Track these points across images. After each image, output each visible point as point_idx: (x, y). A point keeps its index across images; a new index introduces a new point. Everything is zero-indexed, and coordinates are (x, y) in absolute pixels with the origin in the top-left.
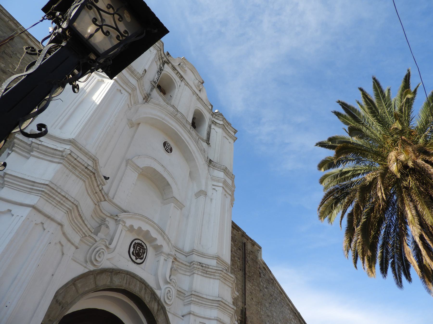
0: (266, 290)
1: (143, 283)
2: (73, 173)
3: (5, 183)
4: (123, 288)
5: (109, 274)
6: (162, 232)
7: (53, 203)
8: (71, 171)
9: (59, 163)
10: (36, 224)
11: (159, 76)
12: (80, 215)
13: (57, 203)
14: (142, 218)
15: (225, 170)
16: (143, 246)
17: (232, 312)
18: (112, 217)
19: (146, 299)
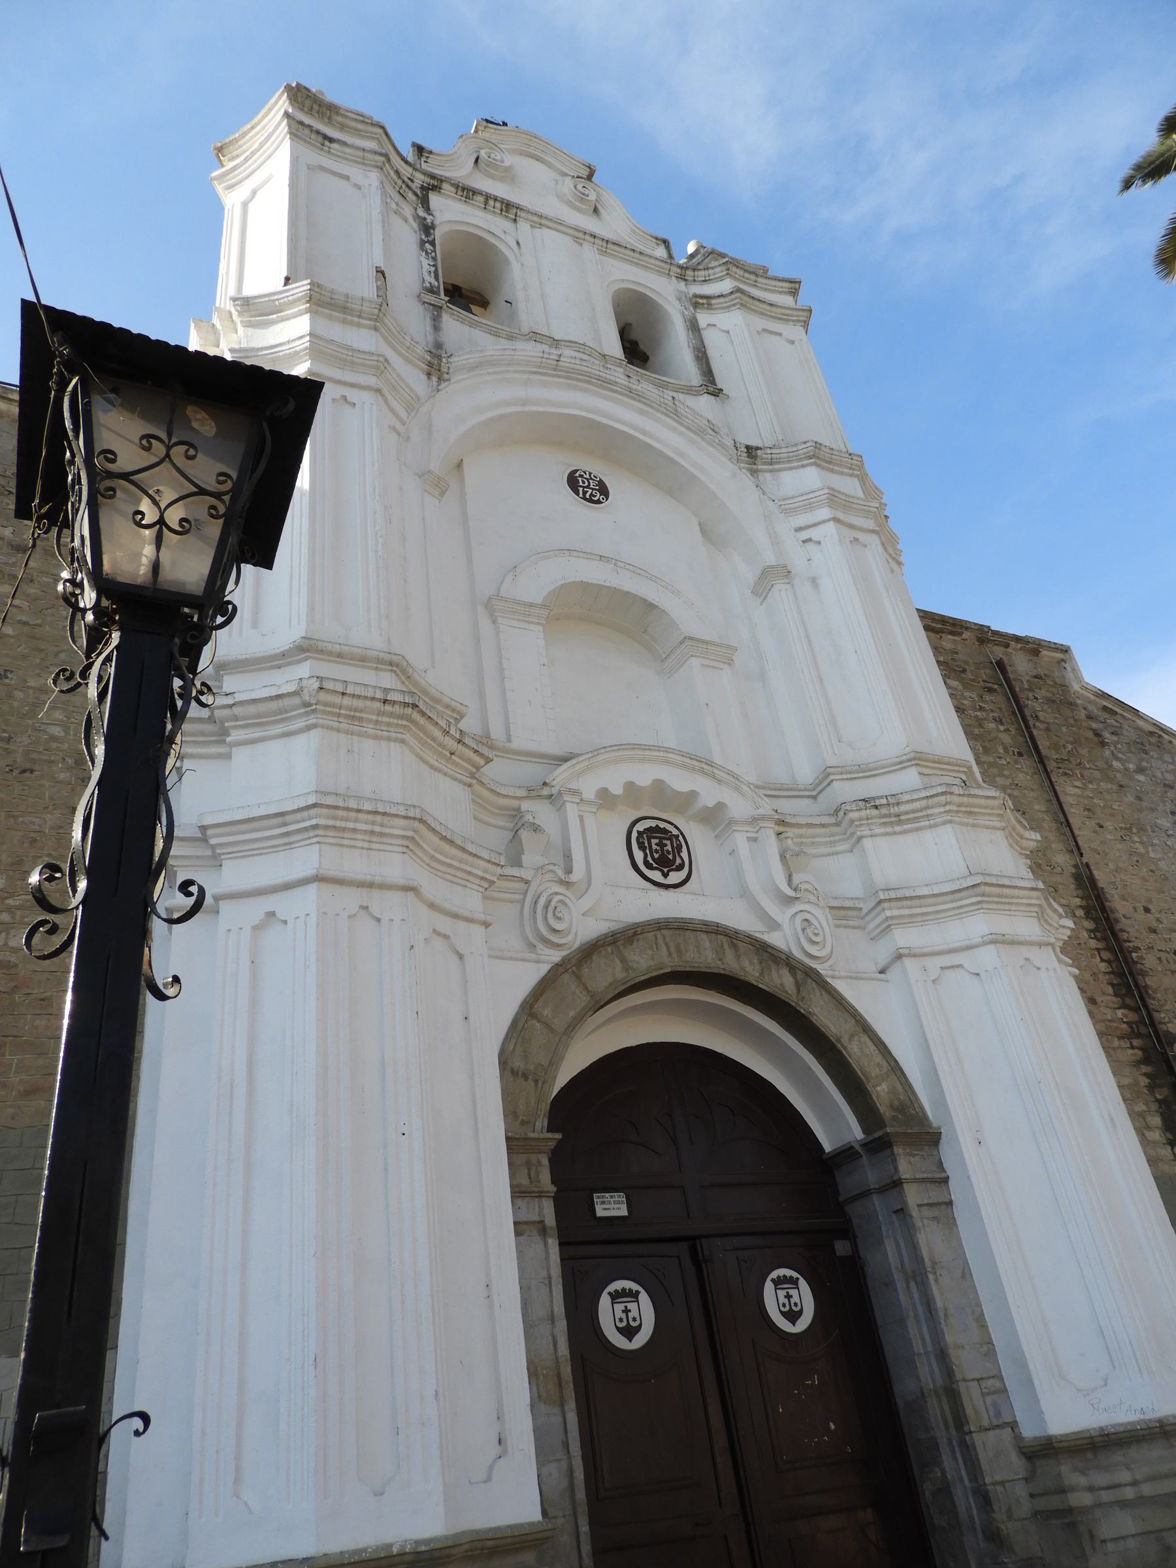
0: (1141, 778)
1: (717, 933)
2: (360, 735)
3: (218, 851)
4: (668, 970)
5: (609, 949)
6: (704, 765)
7: (360, 844)
8: (352, 734)
9: (309, 728)
10: (349, 917)
11: (434, 259)
12: (444, 838)
13: (367, 838)
14: (621, 753)
15: (819, 456)
16: (665, 831)
17: (1036, 899)
18: (535, 793)
19: (749, 970)
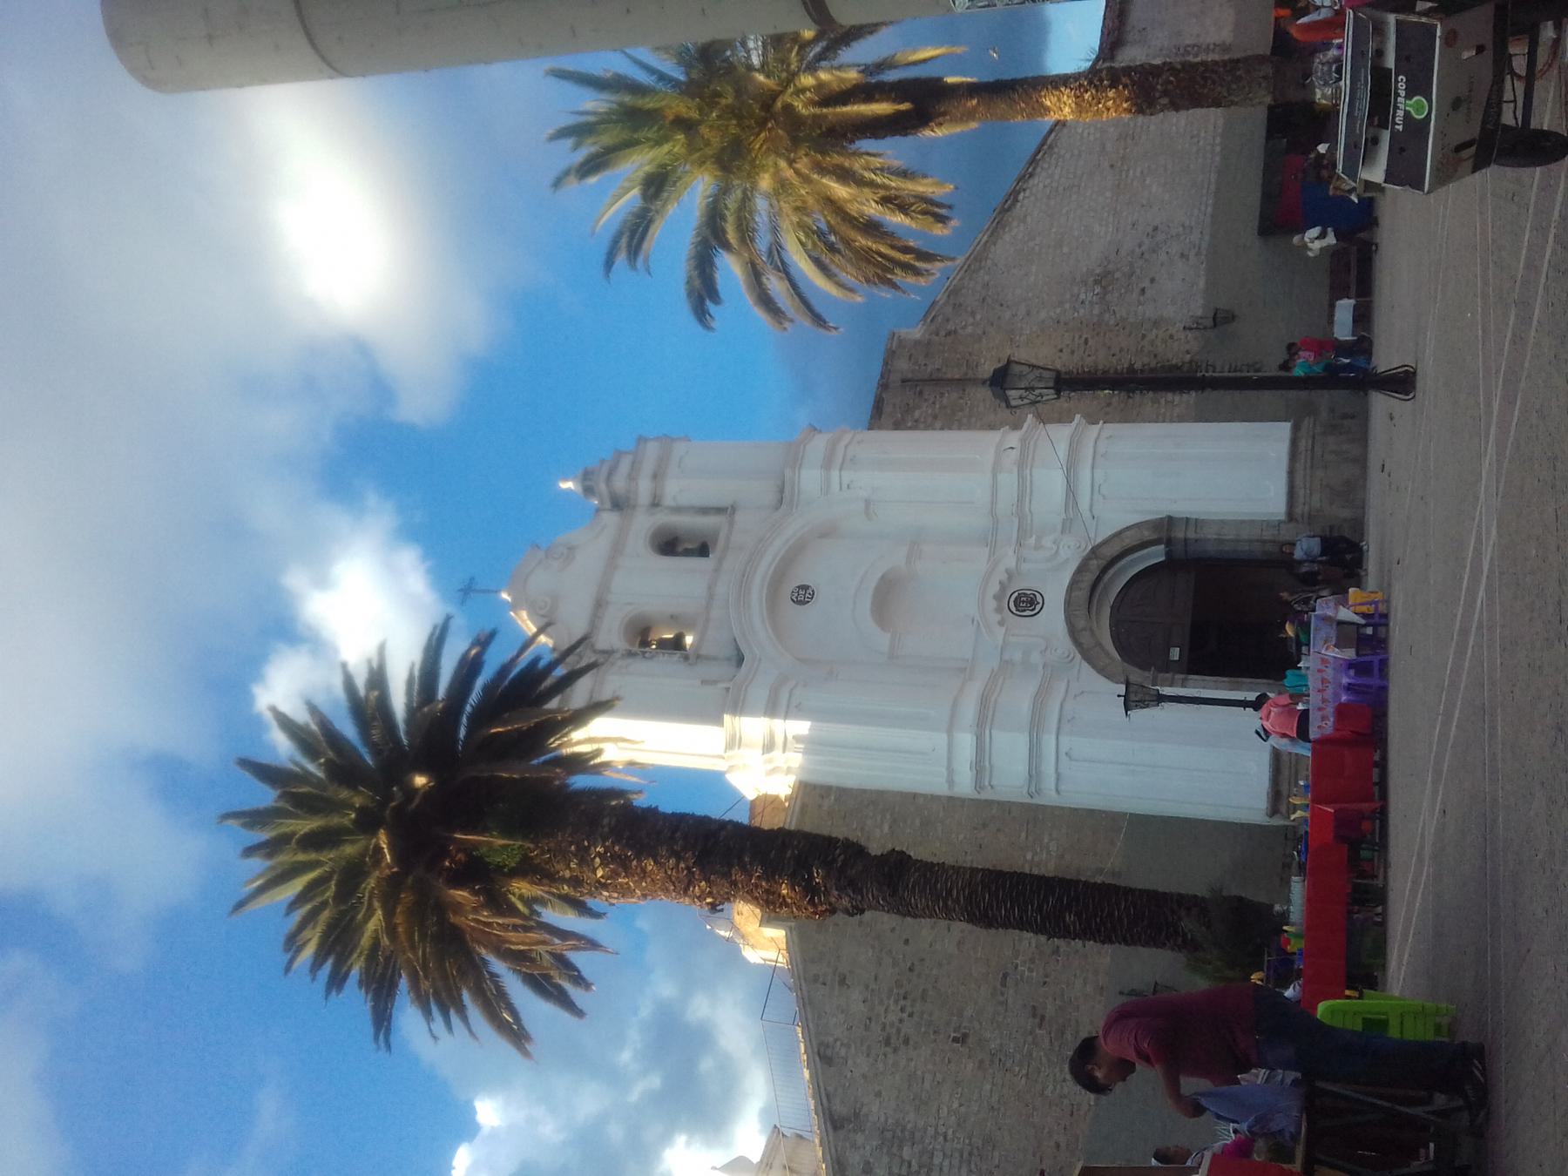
0: (978, 317)
19: (1089, 578)
